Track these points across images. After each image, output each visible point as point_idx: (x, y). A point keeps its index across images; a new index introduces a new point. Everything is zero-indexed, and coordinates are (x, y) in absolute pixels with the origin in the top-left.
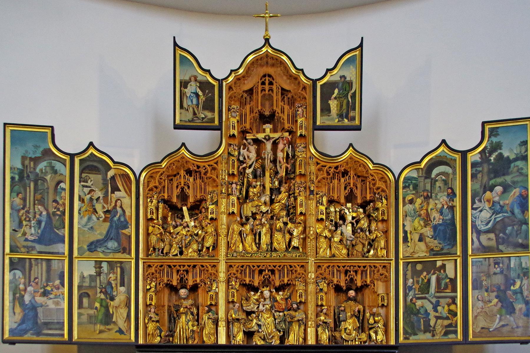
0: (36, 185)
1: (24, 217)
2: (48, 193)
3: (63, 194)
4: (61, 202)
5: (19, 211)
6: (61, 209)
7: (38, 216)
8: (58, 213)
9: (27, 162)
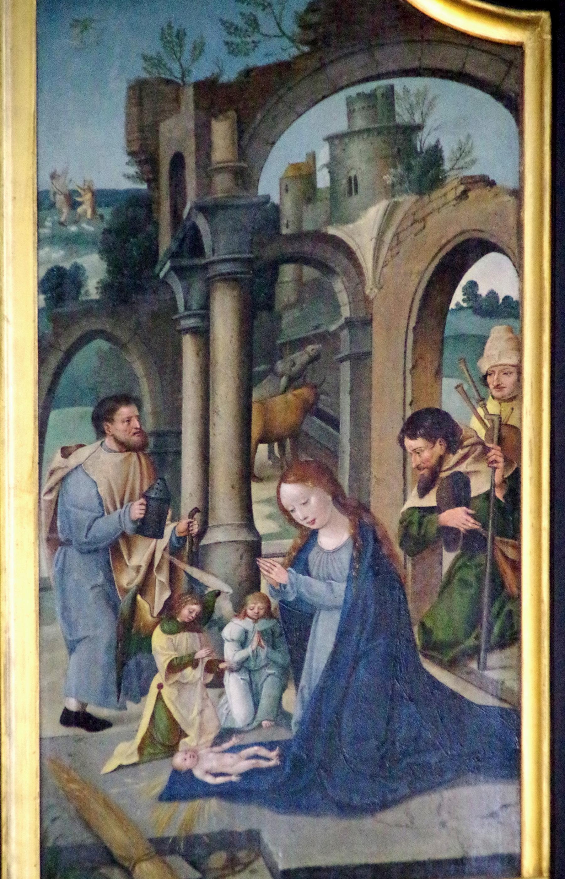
0: (257, 306)
1: (161, 595)
2: (361, 359)
3: (496, 351)
4: (475, 427)
5: (111, 552)
6: (479, 486)
7: (274, 573)
8: (458, 518)
9: (176, 131)
